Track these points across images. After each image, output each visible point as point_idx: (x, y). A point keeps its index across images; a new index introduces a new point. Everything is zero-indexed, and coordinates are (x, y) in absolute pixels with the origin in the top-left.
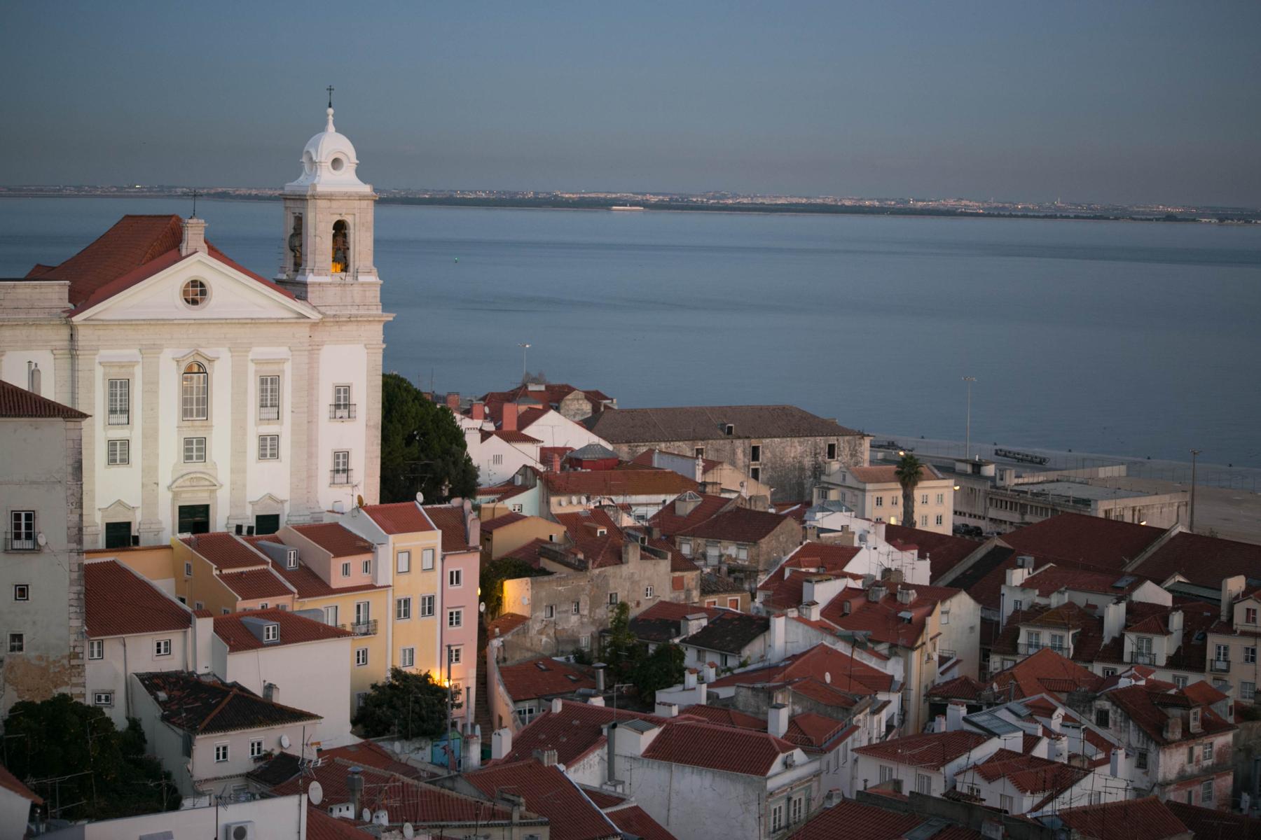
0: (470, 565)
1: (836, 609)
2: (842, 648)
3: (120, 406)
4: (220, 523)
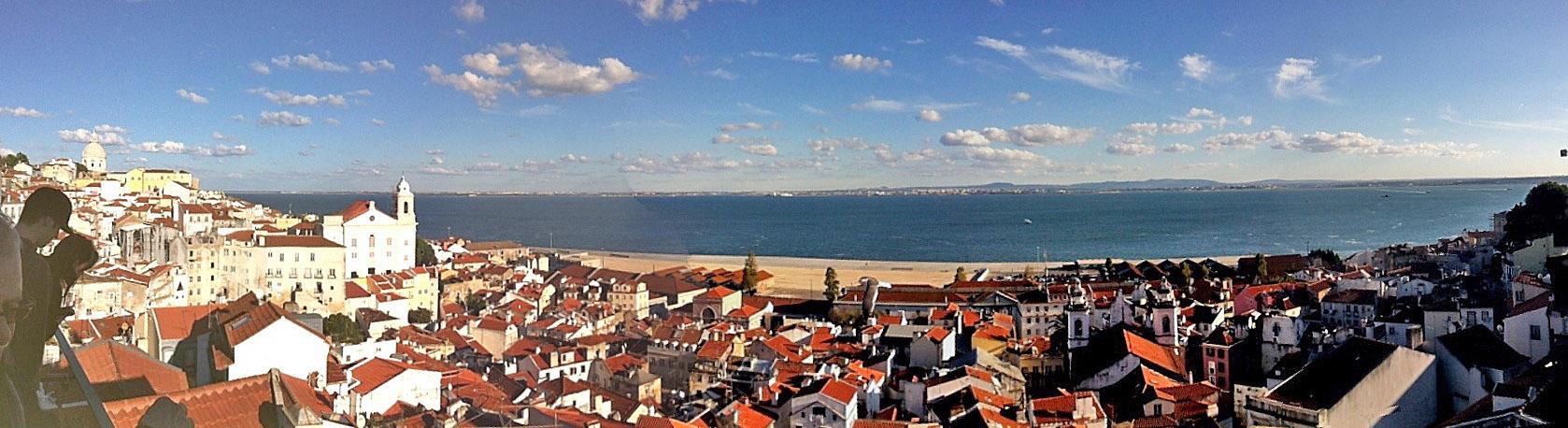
0: (436, 281)
1: (522, 289)
2: (523, 299)
3: (354, 243)
4: (377, 273)
